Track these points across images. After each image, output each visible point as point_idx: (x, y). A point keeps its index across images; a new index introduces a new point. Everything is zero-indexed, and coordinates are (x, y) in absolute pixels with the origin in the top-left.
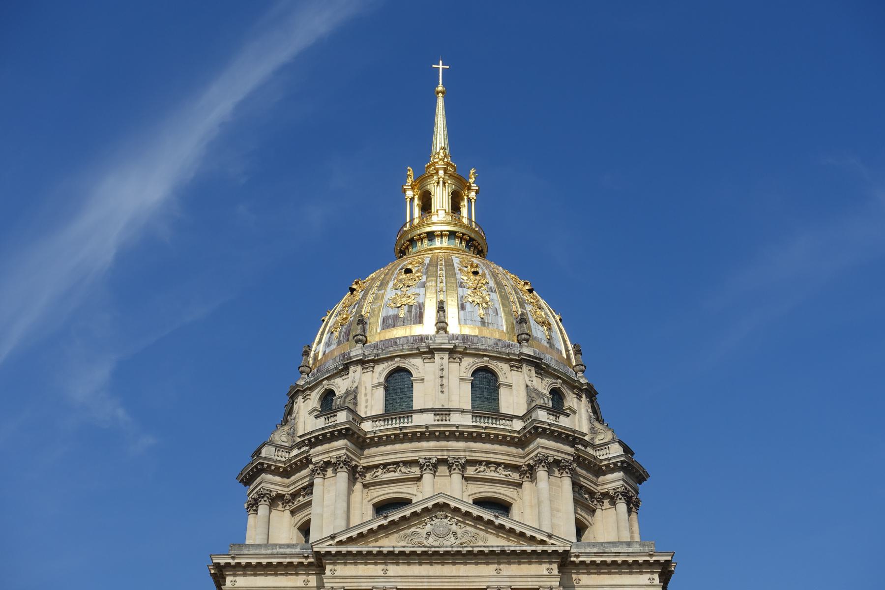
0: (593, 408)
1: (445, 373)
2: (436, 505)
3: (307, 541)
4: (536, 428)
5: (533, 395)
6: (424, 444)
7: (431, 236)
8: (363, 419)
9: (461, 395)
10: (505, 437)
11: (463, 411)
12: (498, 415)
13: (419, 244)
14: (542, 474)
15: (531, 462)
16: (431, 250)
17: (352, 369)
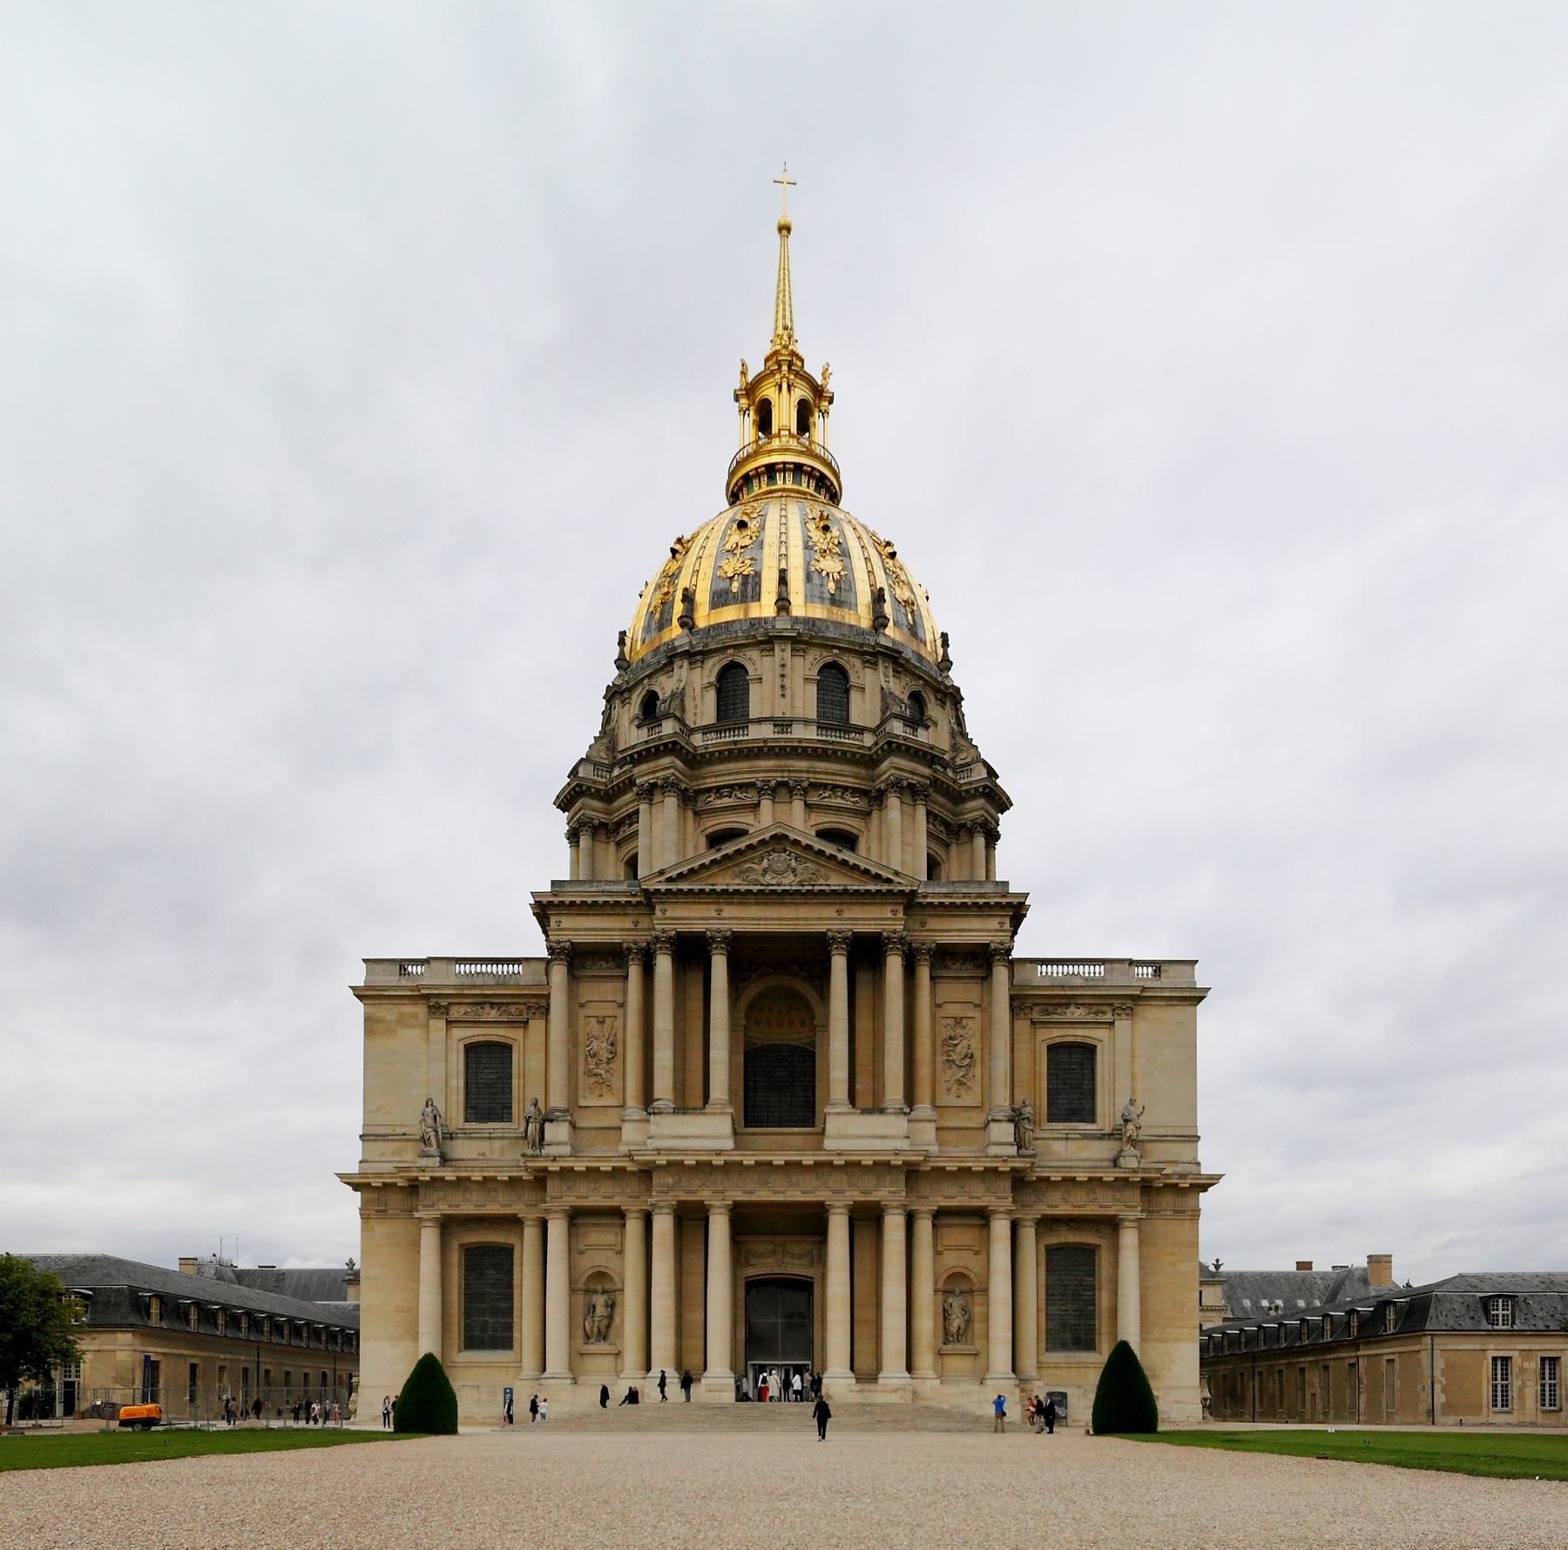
0: (957, 717)
1: (788, 671)
2: (773, 837)
3: (635, 877)
4: (890, 743)
5: (889, 700)
6: (763, 764)
7: (771, 470)
8: (692, 731)
9: (805, 701)
10: (854, 754)
11: (806, 722)
12: (848, 728)
13: (755, 483)
14: (893, 802)
15: (883, 786)
16: (771, 492)
17: (677, 663)
